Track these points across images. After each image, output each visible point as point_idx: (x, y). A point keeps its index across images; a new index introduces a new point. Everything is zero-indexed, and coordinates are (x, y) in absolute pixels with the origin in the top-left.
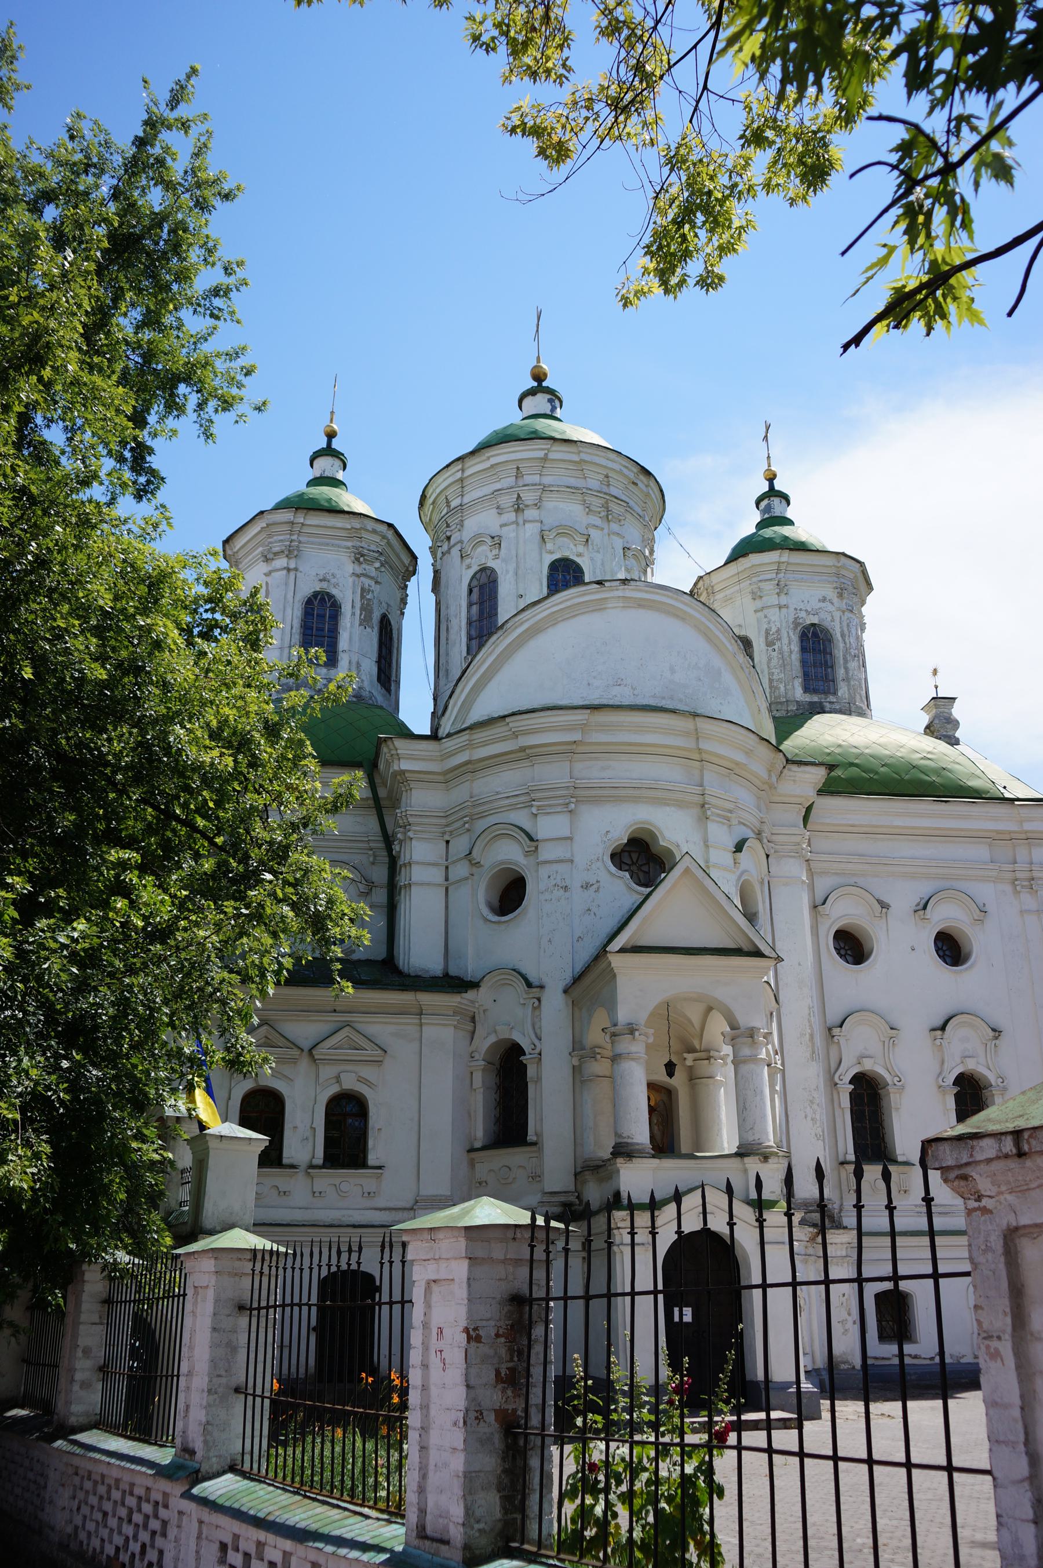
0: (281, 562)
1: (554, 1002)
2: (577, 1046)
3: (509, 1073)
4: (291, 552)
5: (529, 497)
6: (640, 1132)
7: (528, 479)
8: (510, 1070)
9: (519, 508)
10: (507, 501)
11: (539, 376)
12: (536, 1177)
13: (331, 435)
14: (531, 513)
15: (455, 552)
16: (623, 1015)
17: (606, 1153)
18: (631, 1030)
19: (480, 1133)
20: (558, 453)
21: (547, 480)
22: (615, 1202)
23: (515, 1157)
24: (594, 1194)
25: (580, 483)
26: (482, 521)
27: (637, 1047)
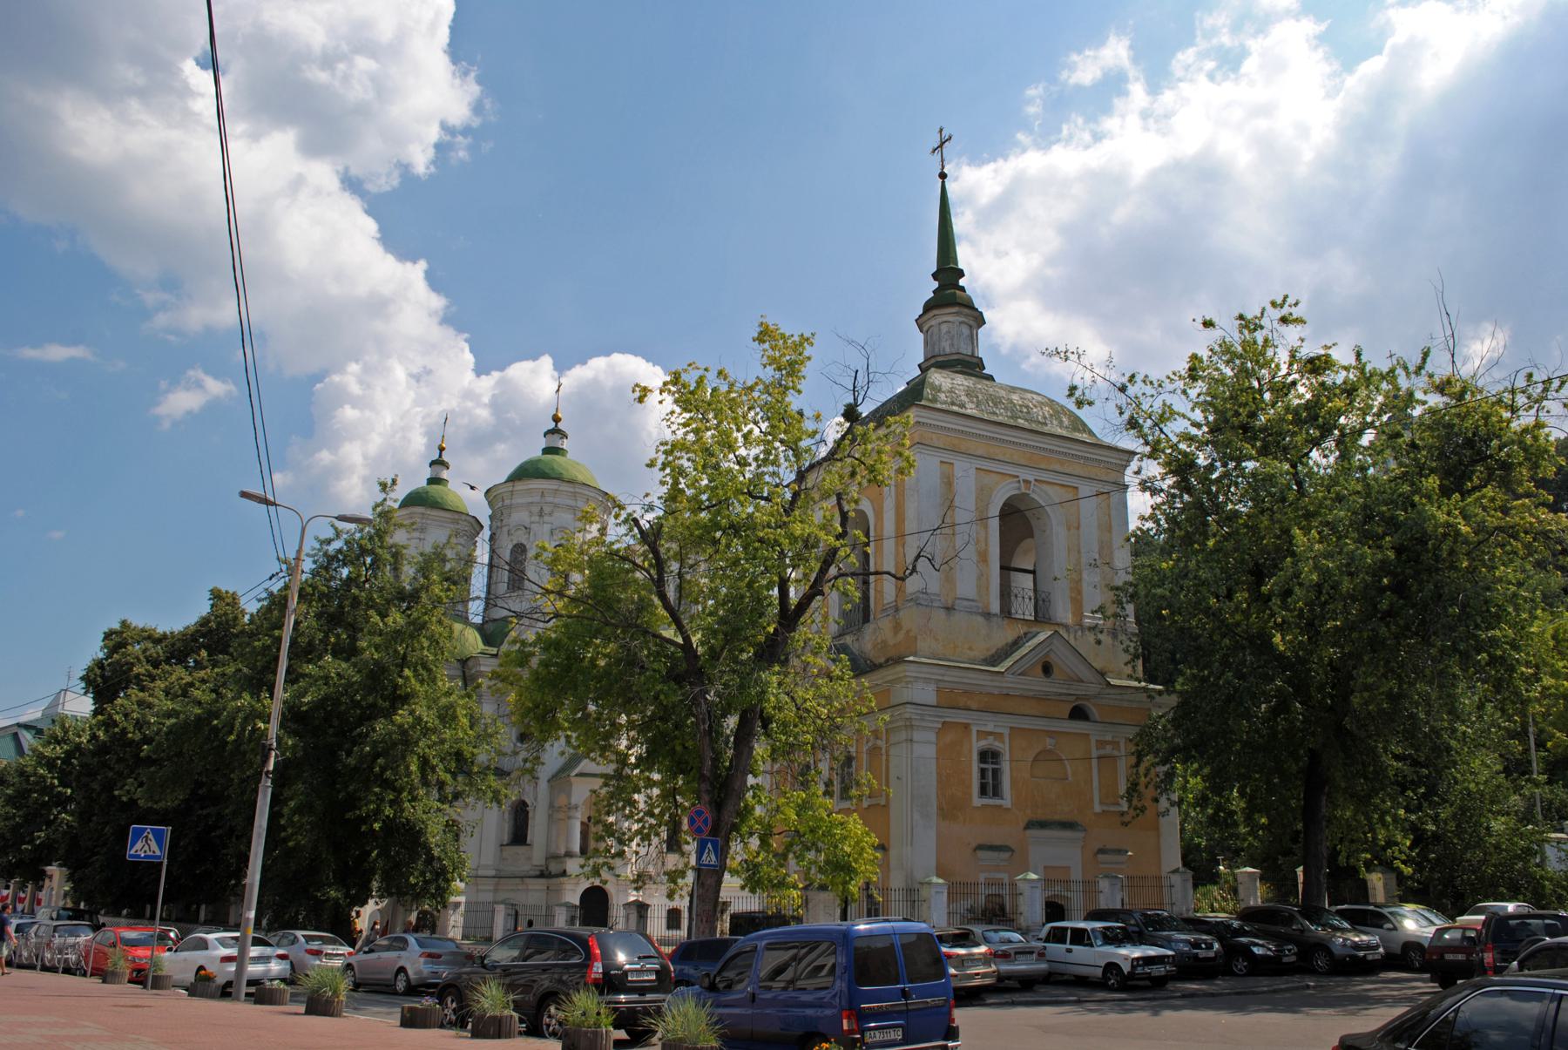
0: (416, 534)
1: (543, 785)
2: (551, 806)
3: (520, 814)
4: (422, 530)
5: (547, 509)
6: (576, 848)
7: (550, 499)
8: (520, 814)
9: (541, 514)
10: (536, 509)
11: (556, 419)
12: (529, 859)
13: (442, 449)
14: (546, 518)
15: (505, 529)
16: (574, 801)
17: (562, 852)
18: (576, 807)
19: (506, 839)
20: (565, 487)
21: (556, 501)
22: (564, 873)
23: (520, 849)
24: (554, 867)
25: (572, 503)
26: (519, 517)
27: (578, 815)
